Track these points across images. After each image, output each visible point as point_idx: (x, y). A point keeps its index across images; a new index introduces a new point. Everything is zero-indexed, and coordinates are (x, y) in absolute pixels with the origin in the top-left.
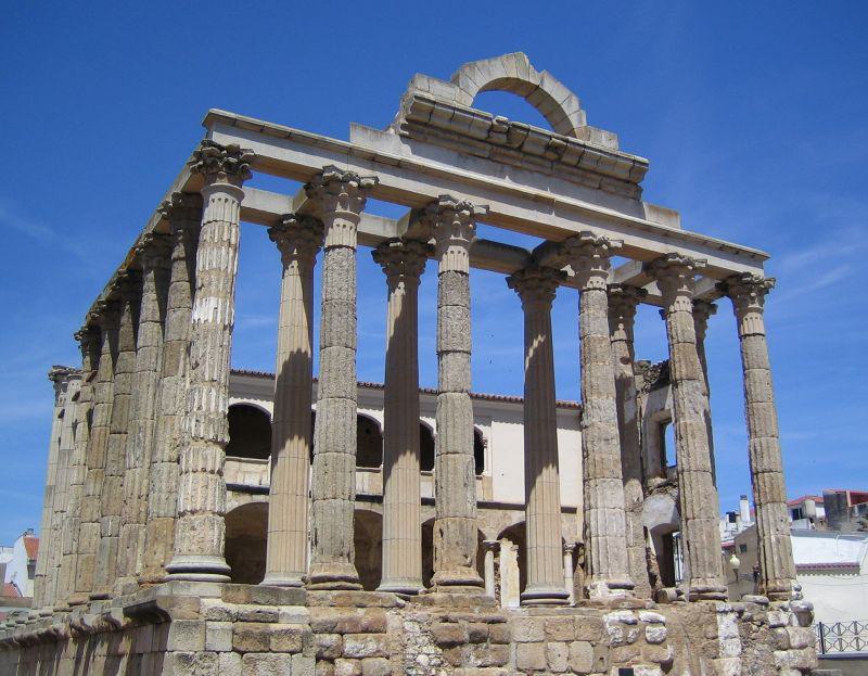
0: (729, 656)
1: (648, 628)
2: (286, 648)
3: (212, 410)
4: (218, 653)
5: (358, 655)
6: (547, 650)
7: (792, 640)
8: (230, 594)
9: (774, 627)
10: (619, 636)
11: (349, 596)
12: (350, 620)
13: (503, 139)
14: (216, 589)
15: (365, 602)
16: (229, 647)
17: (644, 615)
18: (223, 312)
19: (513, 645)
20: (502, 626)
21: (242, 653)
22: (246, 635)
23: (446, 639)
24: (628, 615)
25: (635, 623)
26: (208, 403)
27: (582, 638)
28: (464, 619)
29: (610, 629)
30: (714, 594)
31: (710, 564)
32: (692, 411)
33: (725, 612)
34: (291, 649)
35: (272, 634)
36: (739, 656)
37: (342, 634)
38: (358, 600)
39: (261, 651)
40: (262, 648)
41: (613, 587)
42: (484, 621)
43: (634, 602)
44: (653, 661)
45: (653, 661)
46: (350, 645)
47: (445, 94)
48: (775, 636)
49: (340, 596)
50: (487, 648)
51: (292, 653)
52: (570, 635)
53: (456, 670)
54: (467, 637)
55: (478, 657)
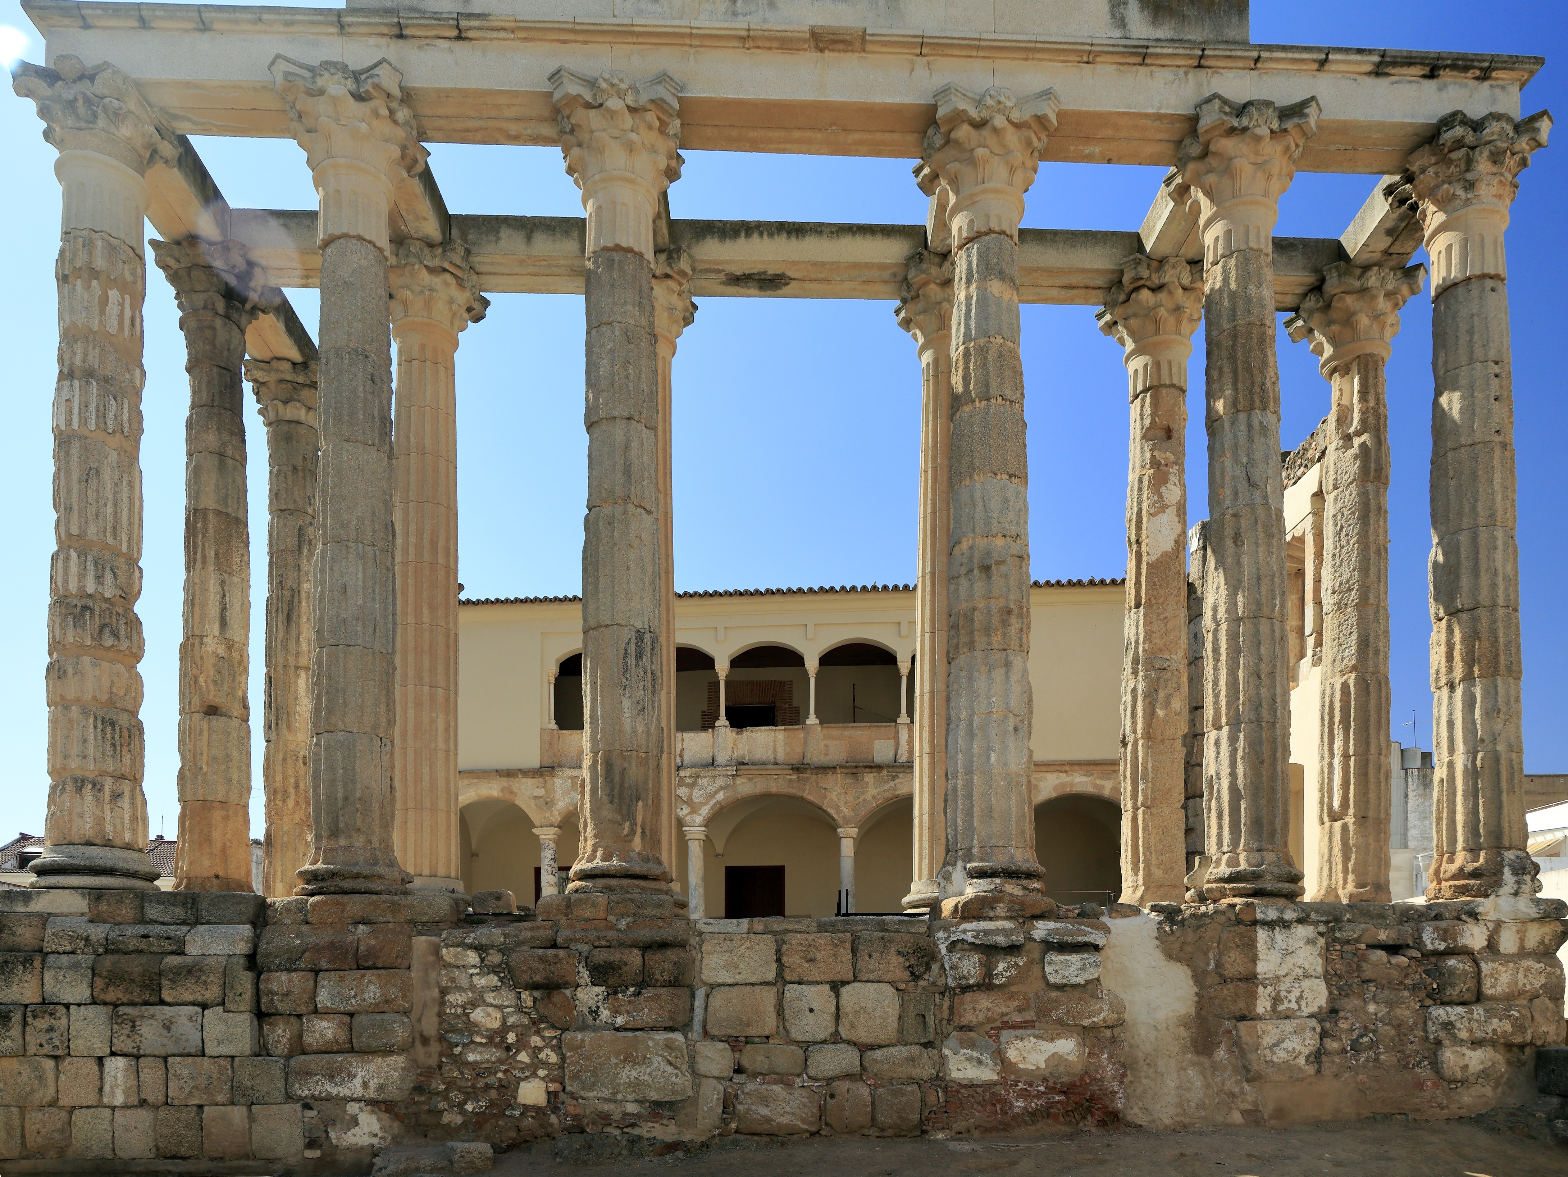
0: (1287, 1016)
7: (1487, 983)
9: (1436, 953)
11: (338, 903)
17: (1042, 929)
19: (700, 994)
23: (538, 978)
27: (872, 977)
37: (317, 972)
44: (1061, 1023)
45: (1061, 1023)
48: (1436, 972)
53: (567, 1036)
54: (585, 975)
55: (616, 1012)
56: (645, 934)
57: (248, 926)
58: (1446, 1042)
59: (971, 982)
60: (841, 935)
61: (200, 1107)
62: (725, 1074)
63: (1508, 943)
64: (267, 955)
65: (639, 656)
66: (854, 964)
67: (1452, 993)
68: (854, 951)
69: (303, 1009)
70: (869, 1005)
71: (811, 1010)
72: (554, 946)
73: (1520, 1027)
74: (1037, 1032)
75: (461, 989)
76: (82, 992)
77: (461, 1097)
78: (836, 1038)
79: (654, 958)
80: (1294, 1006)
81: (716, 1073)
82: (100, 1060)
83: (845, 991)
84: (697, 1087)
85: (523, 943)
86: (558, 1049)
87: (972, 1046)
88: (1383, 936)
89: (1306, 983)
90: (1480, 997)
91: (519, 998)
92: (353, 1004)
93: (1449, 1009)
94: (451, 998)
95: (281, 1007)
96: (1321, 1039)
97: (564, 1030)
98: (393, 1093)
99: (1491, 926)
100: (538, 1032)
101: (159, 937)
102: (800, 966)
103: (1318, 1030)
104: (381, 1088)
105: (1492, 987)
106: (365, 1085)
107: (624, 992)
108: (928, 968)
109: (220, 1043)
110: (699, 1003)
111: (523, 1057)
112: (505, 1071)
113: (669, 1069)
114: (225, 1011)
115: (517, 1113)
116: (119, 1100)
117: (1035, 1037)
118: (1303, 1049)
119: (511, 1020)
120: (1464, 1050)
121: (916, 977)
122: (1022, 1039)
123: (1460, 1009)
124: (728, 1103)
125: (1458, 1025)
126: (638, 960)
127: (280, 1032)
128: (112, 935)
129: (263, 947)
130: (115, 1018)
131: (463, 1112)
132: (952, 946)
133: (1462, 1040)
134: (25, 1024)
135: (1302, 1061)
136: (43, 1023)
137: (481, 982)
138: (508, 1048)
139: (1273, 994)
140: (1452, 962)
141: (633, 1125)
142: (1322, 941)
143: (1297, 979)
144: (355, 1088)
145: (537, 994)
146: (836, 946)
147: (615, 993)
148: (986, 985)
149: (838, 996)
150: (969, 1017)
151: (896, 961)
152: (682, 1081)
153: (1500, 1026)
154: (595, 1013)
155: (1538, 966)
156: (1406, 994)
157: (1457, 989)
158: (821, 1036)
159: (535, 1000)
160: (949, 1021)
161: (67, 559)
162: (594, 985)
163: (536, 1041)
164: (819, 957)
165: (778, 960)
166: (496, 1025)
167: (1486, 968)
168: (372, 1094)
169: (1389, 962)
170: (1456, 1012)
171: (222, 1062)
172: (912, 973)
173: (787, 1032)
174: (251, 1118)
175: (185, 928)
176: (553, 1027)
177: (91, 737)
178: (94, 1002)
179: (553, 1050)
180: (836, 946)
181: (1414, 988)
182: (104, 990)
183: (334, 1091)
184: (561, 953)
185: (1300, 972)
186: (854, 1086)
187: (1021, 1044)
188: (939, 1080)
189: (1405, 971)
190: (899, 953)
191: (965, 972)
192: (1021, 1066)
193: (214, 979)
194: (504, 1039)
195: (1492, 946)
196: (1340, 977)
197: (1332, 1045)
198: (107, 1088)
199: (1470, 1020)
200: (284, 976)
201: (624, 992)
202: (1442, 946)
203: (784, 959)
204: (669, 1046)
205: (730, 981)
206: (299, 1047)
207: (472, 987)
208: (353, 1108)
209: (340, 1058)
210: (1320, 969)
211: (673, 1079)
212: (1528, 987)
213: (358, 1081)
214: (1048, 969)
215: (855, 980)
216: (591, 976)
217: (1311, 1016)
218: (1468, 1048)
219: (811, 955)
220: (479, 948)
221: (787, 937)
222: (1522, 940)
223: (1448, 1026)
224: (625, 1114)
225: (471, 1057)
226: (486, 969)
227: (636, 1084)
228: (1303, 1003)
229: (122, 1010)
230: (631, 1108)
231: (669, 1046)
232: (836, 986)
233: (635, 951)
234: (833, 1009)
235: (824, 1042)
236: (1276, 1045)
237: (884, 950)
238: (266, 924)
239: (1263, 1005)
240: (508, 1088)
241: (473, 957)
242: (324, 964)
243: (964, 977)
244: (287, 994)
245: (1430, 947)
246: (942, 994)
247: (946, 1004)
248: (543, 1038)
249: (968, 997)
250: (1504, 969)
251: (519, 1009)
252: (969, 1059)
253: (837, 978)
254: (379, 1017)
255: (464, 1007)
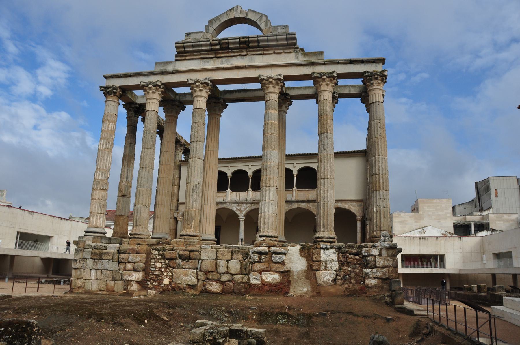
1: (274, 255)
2: (107, 258)
3: (97, 178)
4: (87, 259)
5: (134, 262)
6: (216, 264)
7: (377, 263)
8: (95, 240)
9: (366, 256)
10: (256, 257)
11: (135, 241)
12: (132, 249)
13: (218, 47)
14: (91, 238)
15: (141, 243)
16: (89, 257)
17: (273, 249)
18: (103, 144)
19: (200, 261)
20: (195, 253)
21: (94, 259)
22: (95, 254)
23: (169, 257)
24: (264, 249)
25: (265, 253)
26: (96, 177)
27: (235, 259)
28: (178, 249)
29: (252, 256)
30: (322, 239)
31: (324, 225)
32: (322, 149)
33: (327, 249)
34: (108, 259)
35: (102, 253)
36: (336, 271)
38: (137, 242)
39: (99, 259)
40: (100, 258)
41: (261, 236)
42: (188, 251)
43: (269, 243)
46: (131, 258)
47: (197, 37)
49: (132, 240)
50: (188, 261)
51: (109, 260)
52: (229, 257)
53: (174, 270)
54: (177, 257)
56: (190, 248)
57: (118, 244)
58: (366, 278)
59: (256, 261)
60: (229, 250)
61: (107, 280)
62: (204, 279)
63: (384, 253)
64: (121, 250)
65: (196, 189)
66: (232, 256)
67: (369, 265)
68: (232, 254)
69: (126, 262)
70: (234, 265)
71: (222, 266)
72: (173, 251)
73: (385, 275)
74: (269, 272)
75: (154, 259)
76: (89, 256)
77: (153, 281)
78: (227, 272)
79: (192, 254)
80: (330, 268)
81: (202, 279)
82: (91, 270)
83: (229, 262)
84: (198, 282)
85: (167, 250)
86: (172, 272)
87: (255, 275)
88: (353, 252)
89: (334, 262)
90: (376, 267)
91: (165, 261)
92: (135, 261)
93: (367, 269)
94: (152, 261)
95: (123, 261)
96: (336, 276)
97: (173, 268)
98: (140, 280)
99: (380, 249)
100: (168, 269)
101: (103, 246)
102: (221, 256)
103: (335, 274)
104: (138, 279)
105: (379, 264)
106: (135, 278)
107: (185, 261)
108: (247, 258)
109: (111, 268)
110: (200, 264)
111: (165, 274)
112: (161, 277)
113: (193, 278)
114: (113, 261)
115: (163, 285)
116: (93, 278)
117: (269, 274)
118: (331, 278)
119: (163, 266)
120: (371, 279)
121: (244, 260)
122: (266, 274)
123: (370, 270)
124: (204, 286)
125: (369, 273)
126: (189, 253)
127: (122, 266)
128: (96, 245)
129: (120, 248)
130: (94, 262)
131: (153, 285)
132: (253, 253)
133: (370, 277)
134: (80, 262)
135: (330, 281)
136: (82, 262)
137: (158, 257)
138: (162, 271)
139: (325, 265)
140: (369, 258)
141: (185, 290)
142: (337, 253)
143: (331, 261)
144: (133, 278)
145: (168, 260)
146: (228, 252)
147: (183, 261)
148: (259, 262)
149: (228, 263)
150: (255, 269)
151: (240, 255)
152: (194, 281)
153: (379, 274)
154: (179, 265)
155: (390, 259)
156: (358, 266)
157: (370, 265)
158: (224, 272)
159: (168, 262)
160: (251, 269)
161: (97, 172)
162: (179, 259)
163: (168, 270)
164: (224, 254)
165: (216, 255)
166: (160, 267)
167: (377, 259)
168: (136, 280)
169: (354, 258)
170: (369, 270)
171: (111, 272)
172: (244, 259)
173: (217, 271)
174: (115, 283)
175: (108, 244)
176: (171, 267)
177: (97, 206)
178: (91, 258)
179: (171, 272)
180: (228, 252)
181: (359, 264)
182: (93, 256)
183: (130, 279)
184: (174, 252)
185: (331, 260)
186: (229, 283)
187: (266, 275)
188: (248, 283)
189: (358, 260)
190: (241, 254)
191: (255, 259)
192: (266, 280)
193: (111, 255)
194: (161, 270)
195: (380, 255)
196: (342, 262)
197: (338, 277)
198: (91, 276)
199: (372, 273)
200: (123, 255)
201: (185, 261)
202: (367, 254)
203: (217, 255)
204: (193, 273)
205: (206, 259)
206: (125, 270)
207: (156, 258)
208: (132, 283)
209: (131, 272)
210: (337, 259)
211: (193, 280)
212: (388, 264)
213: (134, 277)
214: (273, 258)
215: (232, 259)
216: (179, 257)
217: (334, 270)
218: (372, 279)
219: (223, 254)
220: (159, 251)
221: (218, 250)
222: (388, 253)
223: (366, 274)
224: (183, 287)
225: (155, 273)
226: (159, 255)
227: (186, 280)
228: (332, 268)
229: (96, 260)
230: (185, 286)
231: (193, 273)
232: (228, 261)
233: (188, 252)
234: (227, 266)
235: (224, 273)
236: (324, 277)
237: (238, 253)
238: (122, 244)
239: (322, 268)
240: (162, 280)
241: (157, 252)
242: (130, 253)
243: (254, 260)
244: (123, 259)
245: (364, 254)
246: (250, 264)
247: (251, 266)
248: (169, 270)
249: (256, 264)
250: (381, 260)
251: (165, 263)
252: (255, 278)
253: (228, 259)
254: (138, 264)
255: (154, 263)
